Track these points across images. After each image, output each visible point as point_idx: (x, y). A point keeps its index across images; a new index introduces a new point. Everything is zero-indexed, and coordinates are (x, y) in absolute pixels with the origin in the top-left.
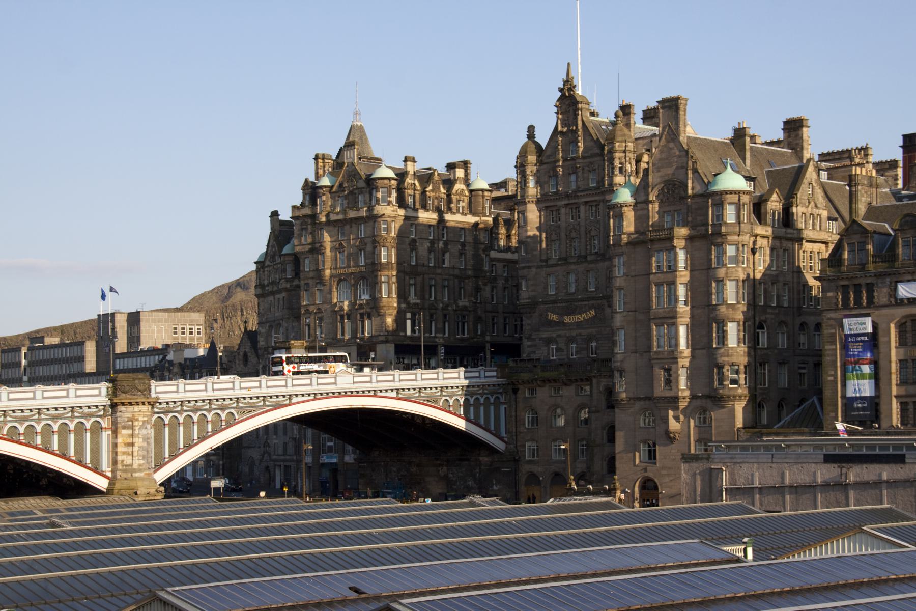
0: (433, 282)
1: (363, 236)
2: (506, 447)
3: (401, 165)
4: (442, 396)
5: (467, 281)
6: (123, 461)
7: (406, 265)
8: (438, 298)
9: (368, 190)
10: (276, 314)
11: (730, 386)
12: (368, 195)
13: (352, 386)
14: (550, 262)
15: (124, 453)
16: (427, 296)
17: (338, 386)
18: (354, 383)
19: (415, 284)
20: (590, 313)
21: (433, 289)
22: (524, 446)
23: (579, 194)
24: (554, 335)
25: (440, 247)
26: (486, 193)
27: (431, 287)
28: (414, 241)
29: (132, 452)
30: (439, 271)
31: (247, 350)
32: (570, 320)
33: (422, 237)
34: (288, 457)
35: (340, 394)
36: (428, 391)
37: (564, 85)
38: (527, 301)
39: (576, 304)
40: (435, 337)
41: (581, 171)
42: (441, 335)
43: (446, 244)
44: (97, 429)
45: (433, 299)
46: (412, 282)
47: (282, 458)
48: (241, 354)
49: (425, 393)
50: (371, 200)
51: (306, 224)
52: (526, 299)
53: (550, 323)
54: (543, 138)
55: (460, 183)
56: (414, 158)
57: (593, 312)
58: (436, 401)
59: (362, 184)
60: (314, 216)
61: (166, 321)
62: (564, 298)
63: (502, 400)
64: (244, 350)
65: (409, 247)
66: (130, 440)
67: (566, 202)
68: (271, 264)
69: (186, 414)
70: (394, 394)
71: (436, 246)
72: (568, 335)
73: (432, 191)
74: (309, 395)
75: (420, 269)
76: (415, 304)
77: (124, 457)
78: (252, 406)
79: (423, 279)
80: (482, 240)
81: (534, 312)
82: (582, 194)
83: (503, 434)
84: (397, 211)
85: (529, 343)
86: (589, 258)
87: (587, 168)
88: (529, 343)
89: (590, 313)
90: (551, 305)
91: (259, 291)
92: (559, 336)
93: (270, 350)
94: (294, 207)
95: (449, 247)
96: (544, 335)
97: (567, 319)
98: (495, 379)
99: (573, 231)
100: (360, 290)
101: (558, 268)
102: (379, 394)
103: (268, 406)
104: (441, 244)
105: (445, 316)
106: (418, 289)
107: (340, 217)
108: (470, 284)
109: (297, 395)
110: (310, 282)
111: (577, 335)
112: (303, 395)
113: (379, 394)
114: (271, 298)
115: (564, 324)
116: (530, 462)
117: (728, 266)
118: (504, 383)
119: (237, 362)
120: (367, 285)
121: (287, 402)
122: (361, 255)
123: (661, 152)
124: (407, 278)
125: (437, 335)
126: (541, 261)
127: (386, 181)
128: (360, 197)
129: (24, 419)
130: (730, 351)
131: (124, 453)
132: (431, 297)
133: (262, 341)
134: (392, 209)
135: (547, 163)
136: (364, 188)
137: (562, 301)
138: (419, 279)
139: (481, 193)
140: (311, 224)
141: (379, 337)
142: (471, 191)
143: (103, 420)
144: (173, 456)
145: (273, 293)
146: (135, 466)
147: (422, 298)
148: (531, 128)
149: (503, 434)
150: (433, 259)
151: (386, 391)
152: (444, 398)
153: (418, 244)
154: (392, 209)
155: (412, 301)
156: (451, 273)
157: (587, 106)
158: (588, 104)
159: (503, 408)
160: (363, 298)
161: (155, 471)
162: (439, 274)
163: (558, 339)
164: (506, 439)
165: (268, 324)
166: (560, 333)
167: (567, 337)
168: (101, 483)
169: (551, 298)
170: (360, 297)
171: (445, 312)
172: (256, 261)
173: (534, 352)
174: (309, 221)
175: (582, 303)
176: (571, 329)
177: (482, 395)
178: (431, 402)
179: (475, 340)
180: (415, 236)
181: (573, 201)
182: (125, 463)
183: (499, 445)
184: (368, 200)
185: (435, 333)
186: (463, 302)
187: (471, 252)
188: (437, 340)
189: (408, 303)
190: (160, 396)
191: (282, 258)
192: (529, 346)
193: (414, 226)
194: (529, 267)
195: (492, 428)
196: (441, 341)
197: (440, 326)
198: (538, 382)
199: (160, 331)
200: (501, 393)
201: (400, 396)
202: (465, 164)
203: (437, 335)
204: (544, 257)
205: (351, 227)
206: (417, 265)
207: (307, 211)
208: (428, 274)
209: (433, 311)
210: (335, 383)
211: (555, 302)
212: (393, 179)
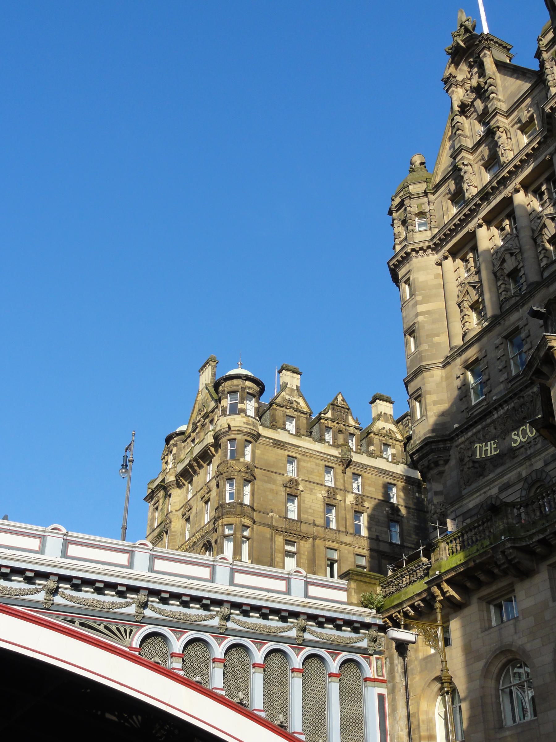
4: (142, 621)
21: (336, 566)
24: (494, 491)
25: (348, 502)
32: (524, 433)
33: (311, 480)
49: (71, 599)
55: (386, 421)
63: (370, 671)
65: (283, 489)
72: (524, 474)
75: (304, 528)
79: (313, 546)
81: (447, 462)
99: (507, 257)
111: (546, 464)
118: (368, 620)
124: (279, 540)
134: (245, 420)
138: (305, 546)
153: (301, 487)
162: (346, 544)
166: (505, 479)
167: (526, 479)
176: (529, 458)
180: (298, 475)
198: (446, 587)
200: (363, 652)
206: (300, 521)
208: (325, 539)
211: (486, 414)
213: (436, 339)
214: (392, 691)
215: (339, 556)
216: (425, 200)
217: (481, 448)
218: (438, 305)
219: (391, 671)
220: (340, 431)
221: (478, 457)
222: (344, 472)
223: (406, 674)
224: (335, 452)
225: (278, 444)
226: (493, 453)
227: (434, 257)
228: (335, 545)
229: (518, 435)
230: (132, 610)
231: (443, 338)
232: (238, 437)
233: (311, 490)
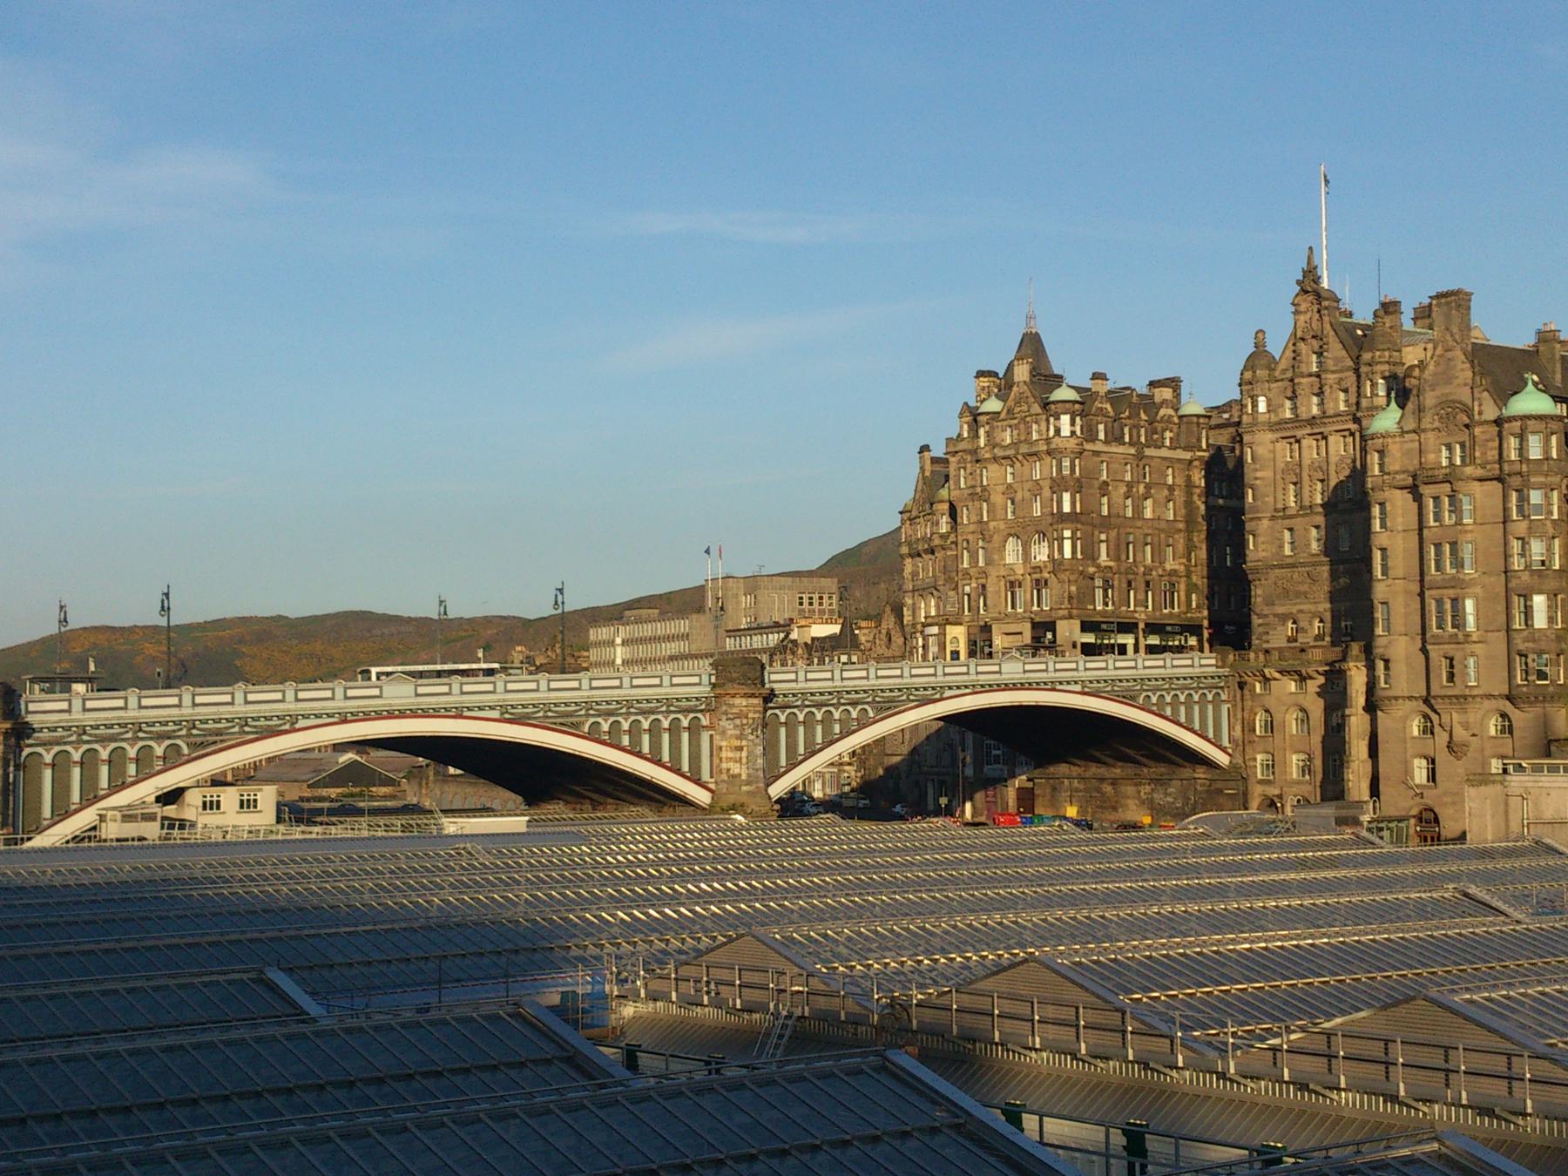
0: (1131, 538)
2: (1231, 762)
3: (1087, 384)
5: (1176, 536)
6: (728, 770)
7: (1094, 515)
8: (1138, 560)
9: (1044, 417)
11: (1538, 682)
12: (1044, 424)
13: (1022, 676)
14: (1289, 512)
15: (729, 759)
16: (1123, 557)
17: (1004, 676)
18: (1025, 672)
19: (1107, 541)
21: (1131, 546)
22: (1255, 760)
23: (1326, 421)
26: (1202, 420)
27: (1128, 544)
28: (1106, 483)
29: (741, 758)
30: (1139, 523)
31: (890, 627)
34: (944, 770)
35: (1006, 687)
36: (1125, 684)
37: (1304, 277)
40: (1135, 611)
41: (1329, 390)
42: (1143, 609)
43: (1148, 487)
44: (695, 729)
45: (1131, 560)
46: (1103, 537)
47: (936, 769)
48: (884, 632)
50: (1048, 430)
51: (965, 461)
54: (1276, 345)
56: (1105, 375)
58: (1133, 698)
59: (1036, 409)
60: (974, 452)
61: (791, 588)
62: (1307, 560)
63: (1224, 697)
66: (738, 743)
69: (807, 710)
70: (1078, 688)
71: (1134, 490)
73: (1129, 418)
74: (966, 687)
76: (1106, 567)
77: (731, 765)
78: (891, 700)
79: (1118, 534)
80: (1197, 483)
82: (1330, 420)
83: (1226, 743)
84: (1082, 444)
85: (1260, 621)
86: (1341, 507)
87: (1335, 386)
88: (1260, 621)
92: (1301, 611)
93: (919, 627)
94: (949, 440)
95: (1153, 491)
96: (1280, 610)
98: (1214, 669)
101: (1299, 519)
102: (1059, 687)
103: (913, 701)
104: (1142, 488)
105: (1147, 584)
106: (1112, 547)
108: (1182, 541)
109: (950, 688)
110: (970, 537)
112: (958, 687)
113: (1059, 687)
116: (1261, 782)
117: (1532, 518)
119: (877, 641)
121: (938, 696)
123: (1437, 364)
125: (1137, 609)
126: (1276, 510)
127: (1068, 405)
128: (1035, 427)
129: (610, 713)
130: (1537, 635)
131: (729, 759)
132: (1128, 558)
135: (1282, 380)
137: (1303, 565)
138: (1113, 533)
139: (1195, 419)
140: (971, 462)
142: (1181, 417)
143: (704, 716)
144: (792, 765)
146: (744, 777)
147: (1118, 559)
148: (1260, 335)
149: (1226, 743)
150: (1130, 508)
151: (1068, 683)
152: (1144, 694)
153: (1110, 488)
154: (1076, 442)
155: (1103, 564)
156: (1156, 524)
157: (1336, 304)
158: (1338, 301)
159: (1225, 708)
160: (1038, 559)
161: (768, 785)
163: (1299, 615)
164: (1230, 751)
166: (1301, 607)
168: (701, 796)
169: (1289, 561)
171: (1148, 578)
172: (901, 509)
173: (1268, 633)
174: (969, 458)
177: (1196, 689)
178: (1128, 699)
179: (1189, 615)
182: (731, 772)
183: (1222, 759)
184: (1044, 430)
185: (1135, 606)
186: (1170, 565)
187: (1182, 499)
188: (1137, 615)
189: (1098, 566)
190: (775, 686)
192: (1259, 625)
193: (1105, 464)
194: (1259, 519)
195: (1211, 735)
196: (1143, 616)
197: (1141, 596)
199: (781, 602)
200: (1222, 688)
201: (1086, 690)
202: (1174, 383)
203: (1137, 609)
204: (1280, 506)
207: (962, 446)
209: (1131, 577)
210: (999, 672)
211: (1293, 566)
212: (1077, 402)
213: (1267, 499)
214: (1235, 706)
215: (1134, 538)
216: (1267, 385)
218: (1268, 474)
219: (1235, 696)
220: (1134, 426)
222: (1138, 466)
223: (1242, 700)
224: (1133, 451)
225: (1096, 453)
227: (1270, 436)
228: (1132, 530)
230: (1138, 687)
231: (1270, 500)
232: (1072, 456)
233: (1117, 487)
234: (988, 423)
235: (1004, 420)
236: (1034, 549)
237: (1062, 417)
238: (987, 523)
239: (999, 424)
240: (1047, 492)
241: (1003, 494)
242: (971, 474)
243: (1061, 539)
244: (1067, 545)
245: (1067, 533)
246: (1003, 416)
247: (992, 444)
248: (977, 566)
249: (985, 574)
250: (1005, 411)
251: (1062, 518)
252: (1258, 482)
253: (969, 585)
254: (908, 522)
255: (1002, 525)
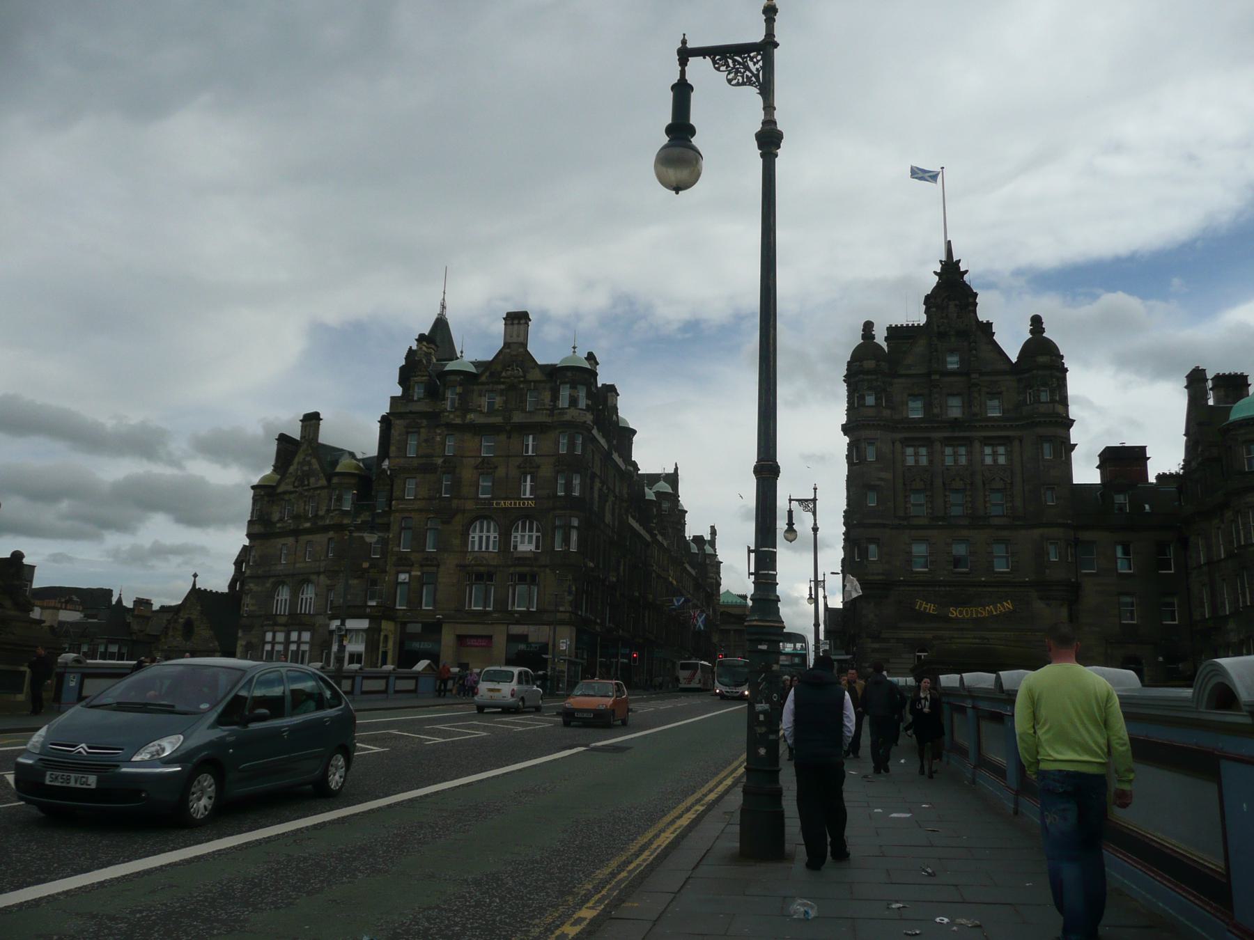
1: (530, 453)
10: (298, 565)
20: (1003, 606)
23: (977, 424)
31: (194, 617)
38: (881, 577)
39: (975, 589)
48: (181, 621)
50: (555, 397)
52: (878, 574)
53: (922, 617)
57: (1008, 605)
60: (434, 418)
64: (186, 616)
67: (946, 435)
68: (290, 488)
85: (876, 646)
88: (876, 646)
89: (1003, 606)
90: (920, 588)
91: (258, 529)
97: (954, 613)
100: (516, 537)
107: (498, 420)
114: (290, 540)
115: (948, 620)
120: (531, 530)
122: (525, 481)
133: (253, 605)
136: (540, 382)
141: (558, 614)
145: (296, 533)
165: (272, 580)
170: (515, 547)
174: (425, 422)
175: (985, 589)
181: (962, 434)
191: (335, 480)
194: (884, 526)
205: (509, 437)
217: (921, 604)
221: (917, 608)
226: (931, 612)
229: (956, 611)
234: (461, 385)
235: (483, 384)
236: (517, 536)
237: (580, 387)
238: (449, 499)
239: (475, 387)
240: (546, 471)
241: (476, 468)
242: (426, 441)
243: (567, 529)
244: (574, 536)
245: (575, 522)
246: (483, 379)
247: (464, 408)
248: (423, 551)
249: (430, 563)
250: (487, 374)
251: (572, 504)
252: (882, 483)
253: (409, 572)
254: (266, 499)
255: (470, 505)
